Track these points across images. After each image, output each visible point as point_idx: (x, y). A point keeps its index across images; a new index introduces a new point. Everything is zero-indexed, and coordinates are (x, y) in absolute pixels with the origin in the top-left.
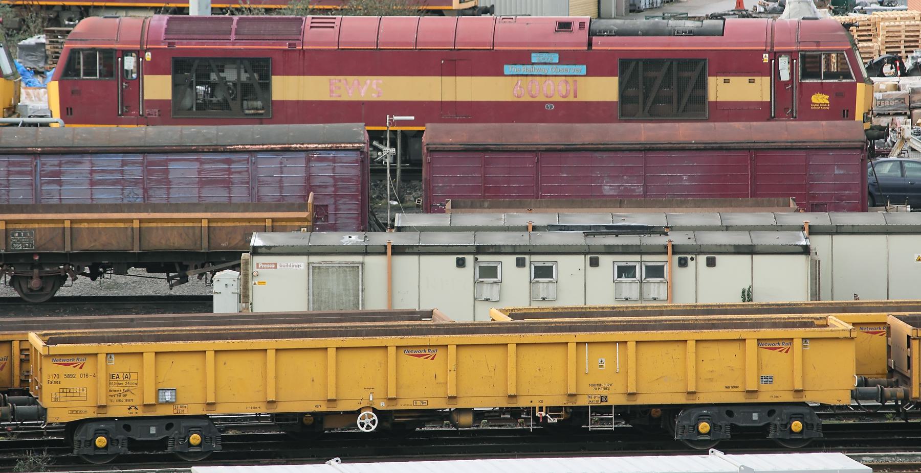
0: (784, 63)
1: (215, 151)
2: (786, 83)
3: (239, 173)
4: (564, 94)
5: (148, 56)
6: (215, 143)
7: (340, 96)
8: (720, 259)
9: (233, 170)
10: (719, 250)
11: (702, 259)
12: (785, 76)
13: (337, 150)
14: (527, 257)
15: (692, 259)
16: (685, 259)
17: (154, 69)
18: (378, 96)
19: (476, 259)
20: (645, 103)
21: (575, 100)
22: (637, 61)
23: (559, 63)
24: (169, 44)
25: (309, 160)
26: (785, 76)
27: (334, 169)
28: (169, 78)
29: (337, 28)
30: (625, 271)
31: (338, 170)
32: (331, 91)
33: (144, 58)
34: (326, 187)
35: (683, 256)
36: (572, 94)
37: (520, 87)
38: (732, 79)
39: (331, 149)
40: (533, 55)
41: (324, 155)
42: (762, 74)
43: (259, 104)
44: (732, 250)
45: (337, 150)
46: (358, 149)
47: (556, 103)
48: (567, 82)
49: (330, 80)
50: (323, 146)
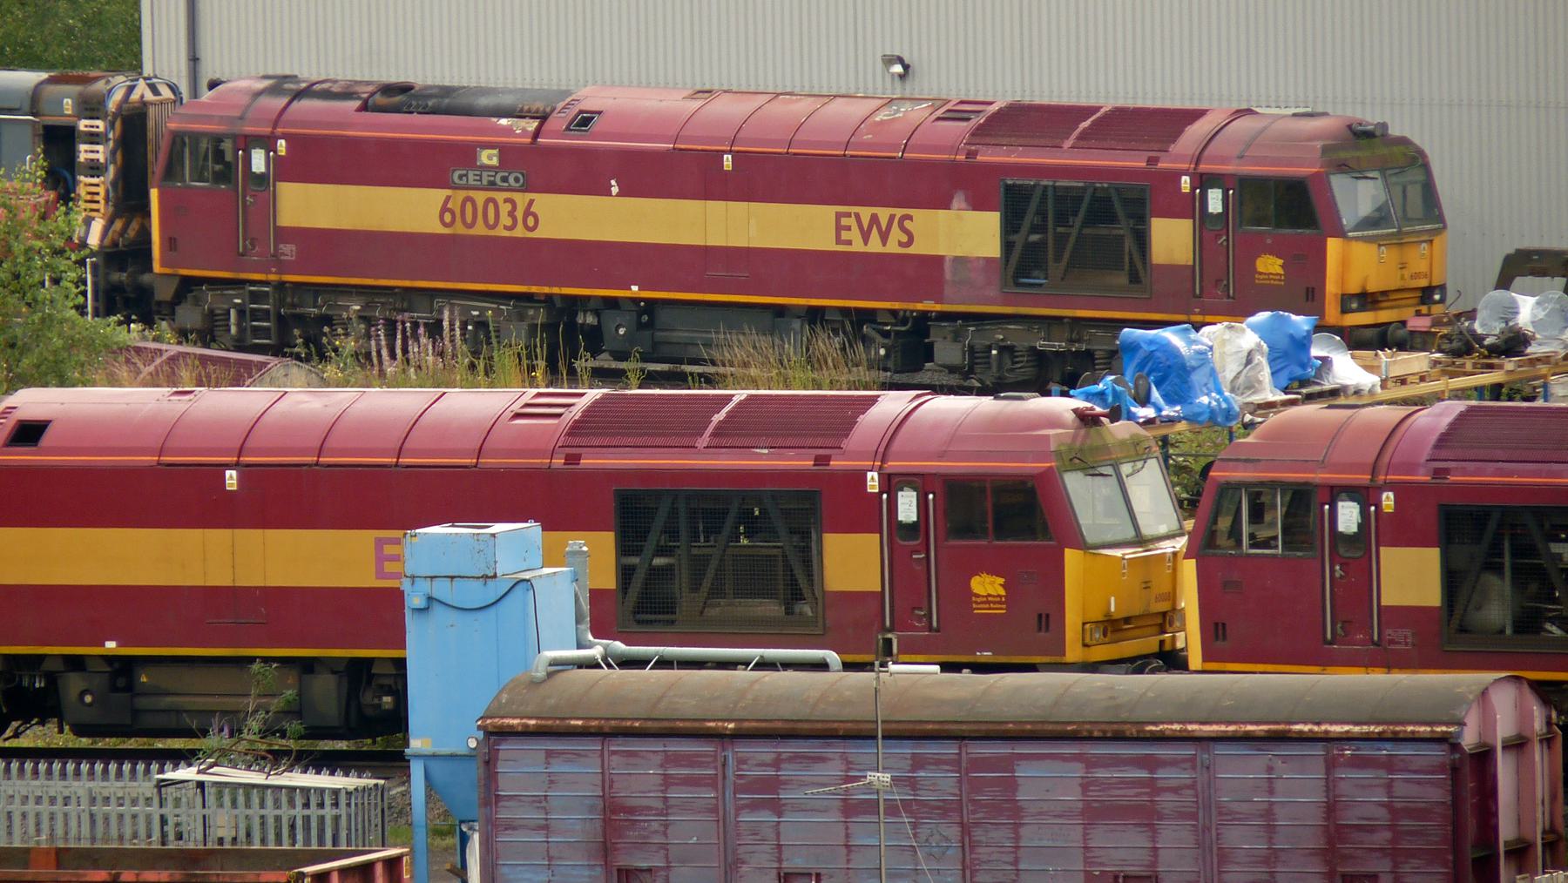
1: (1119, 738)
5: (1388, 500)
13: (1396, 739)
17: (1401, 531)
24: (1438, 473)
25: (1331, 764)
27: (1389, 786)
34: (1371, 829)
39: (1380, 738)
45: (1396, 739)
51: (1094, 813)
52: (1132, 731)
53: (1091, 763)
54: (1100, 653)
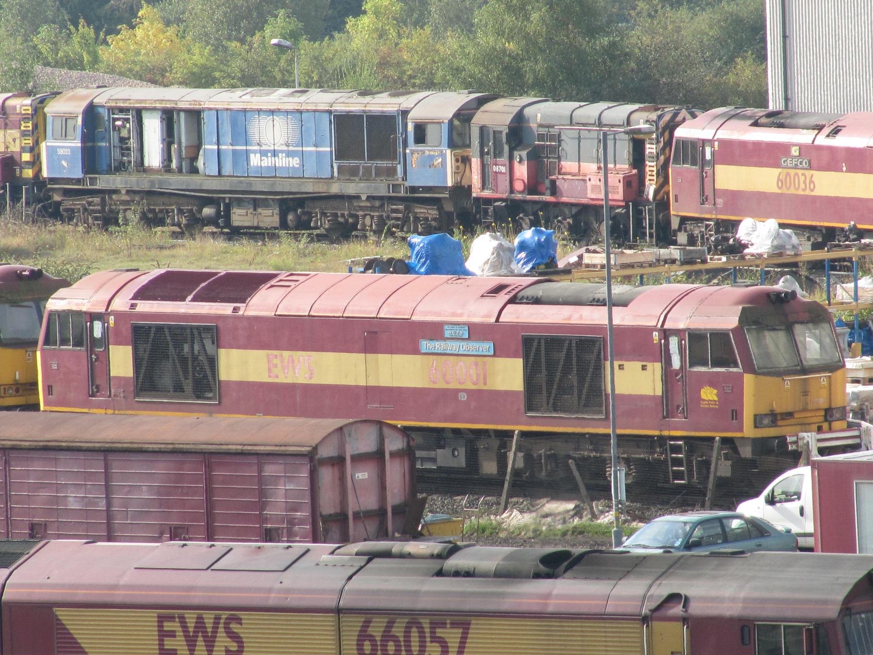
0: (674, 342)
2: (677, 373)
12: (676, 363)
21: (485, 388)
23: (469, 338)
32: (270, 370)
36: (482, 381)
40: (446, 327)
48: (476, 364)
49: (268, 355)
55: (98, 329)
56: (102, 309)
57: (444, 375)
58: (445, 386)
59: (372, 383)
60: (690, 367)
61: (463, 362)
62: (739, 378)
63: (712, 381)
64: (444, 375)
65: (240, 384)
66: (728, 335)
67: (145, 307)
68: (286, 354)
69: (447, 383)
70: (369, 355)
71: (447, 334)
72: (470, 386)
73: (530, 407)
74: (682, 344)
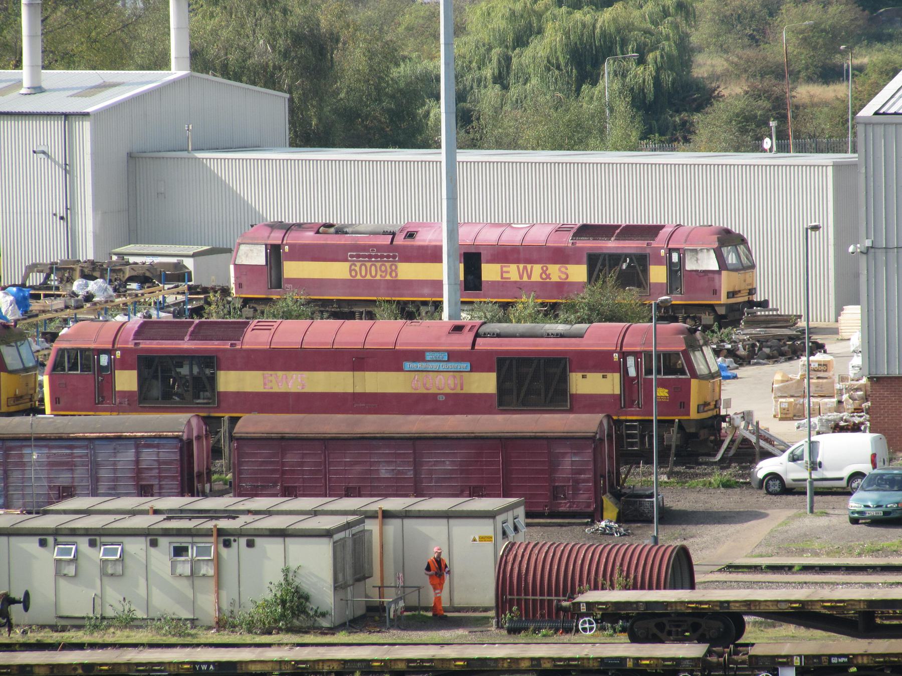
0: (631, 361)
2: (633, 379)
3: (80, 457)
4: (452, 386)
5: (118, 354)
6: (61, 431)
7: (272, 388)
8: (258, 541)
9: (75, 455)
10: (257, 533)
11: (243, 541)
12: (632, 372)
13: (160, 437)
14: (98, 538)
15: (235, 541)
16: (229, 541)
17: (124, 365)
18: (303, 388)
19: (56, 540)
20: (546, 396)
21: (461, 392)
22: (511, 359)
23: (448, 361)
24: (136, 344)
26: (632, 372)
28: (134, 373)
29: (273, 331)
30: (179, 551)
31: (161, 454)
32: (265, 384)
33: (115, 355)
35: (226, 538)
36: (459, 387)
37: (417, 381)
38: (589, 375)
39: (155, 437)
40: (427, 354)
41: (149, 442)
42: (613, 371)
43: (208, 394)
44: (268, 533)
46: (177, 437)
47: (446, 395)
48: (454, 377)
49: (263, 374)
50: (149, 434)
51: (52, 465)
52: (65, 436)
53: (50, 448)
54: (13, 409)
55: (104, 360)
56: (110, 346)
57: (425, 385)
58: (425, 391)
59: (359, 390)
60: (646, 375)
61: (441, 376)
62: (688, 383)
63: (662, 384)
64: (425, 385)
65: (238, 394)
66: (679, 354)
67: (145, 344)
68: (280, 374)
69: (427, 389)
70: (357, 373)
71: (428, 358)
72: (448, 391)
73: (500, 403)
74: (638, 361)
